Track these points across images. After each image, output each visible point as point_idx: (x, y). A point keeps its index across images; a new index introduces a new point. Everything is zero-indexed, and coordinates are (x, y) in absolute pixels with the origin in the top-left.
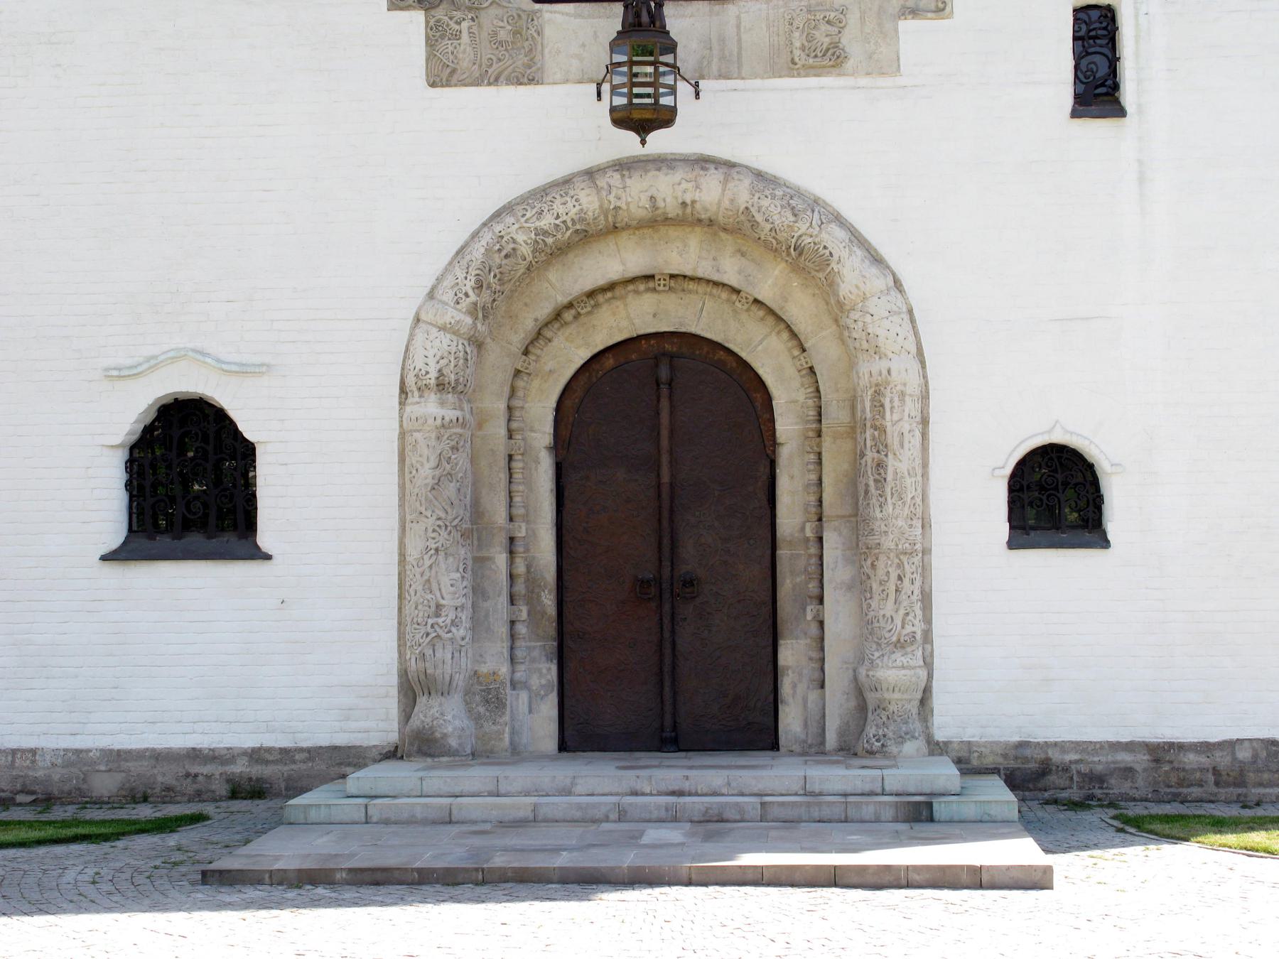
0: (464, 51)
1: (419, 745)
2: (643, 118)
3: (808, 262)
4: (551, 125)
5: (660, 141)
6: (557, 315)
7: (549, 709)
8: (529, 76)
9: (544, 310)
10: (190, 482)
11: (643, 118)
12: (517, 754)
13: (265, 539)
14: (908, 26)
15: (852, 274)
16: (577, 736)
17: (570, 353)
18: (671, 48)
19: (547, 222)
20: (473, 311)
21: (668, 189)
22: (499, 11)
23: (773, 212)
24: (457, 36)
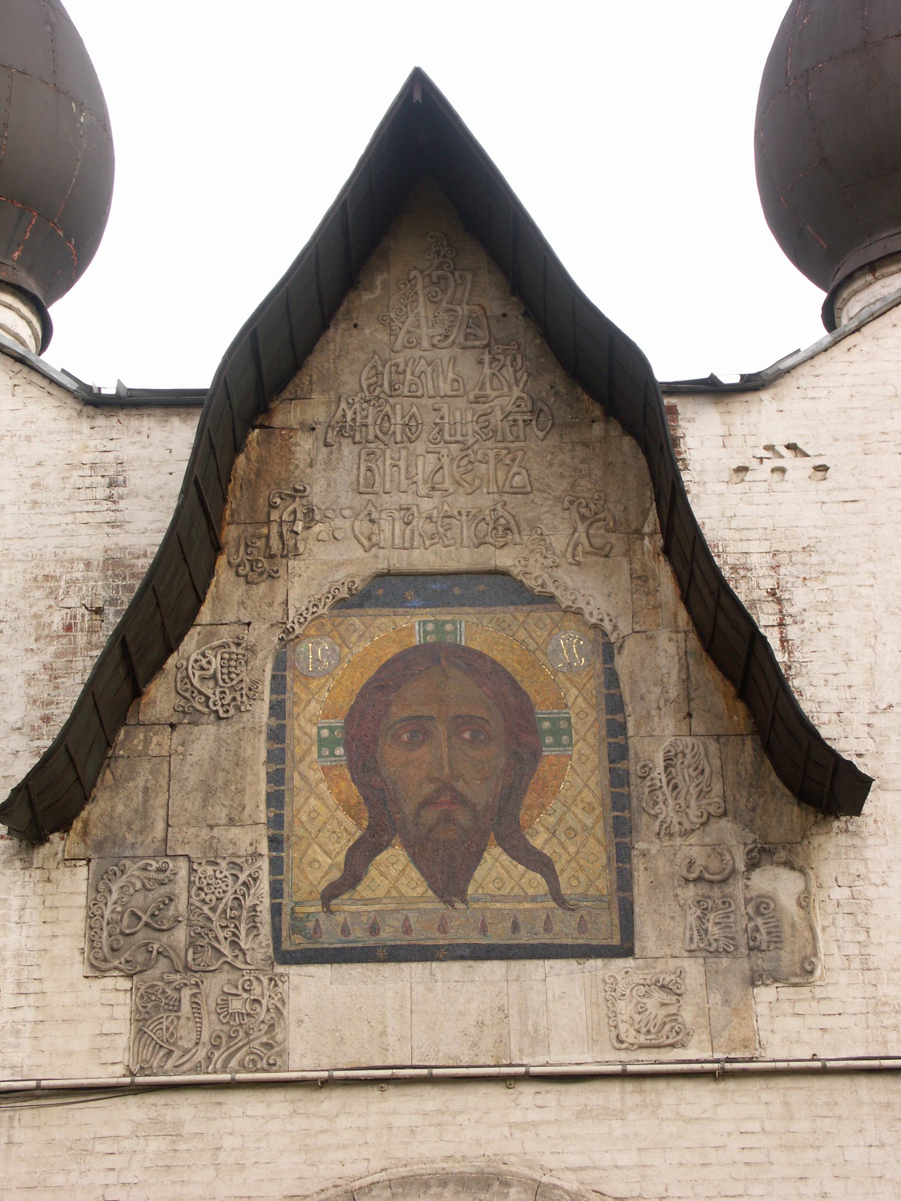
14: (765, 994)
22: (234, 976)
24: (176, 1007)
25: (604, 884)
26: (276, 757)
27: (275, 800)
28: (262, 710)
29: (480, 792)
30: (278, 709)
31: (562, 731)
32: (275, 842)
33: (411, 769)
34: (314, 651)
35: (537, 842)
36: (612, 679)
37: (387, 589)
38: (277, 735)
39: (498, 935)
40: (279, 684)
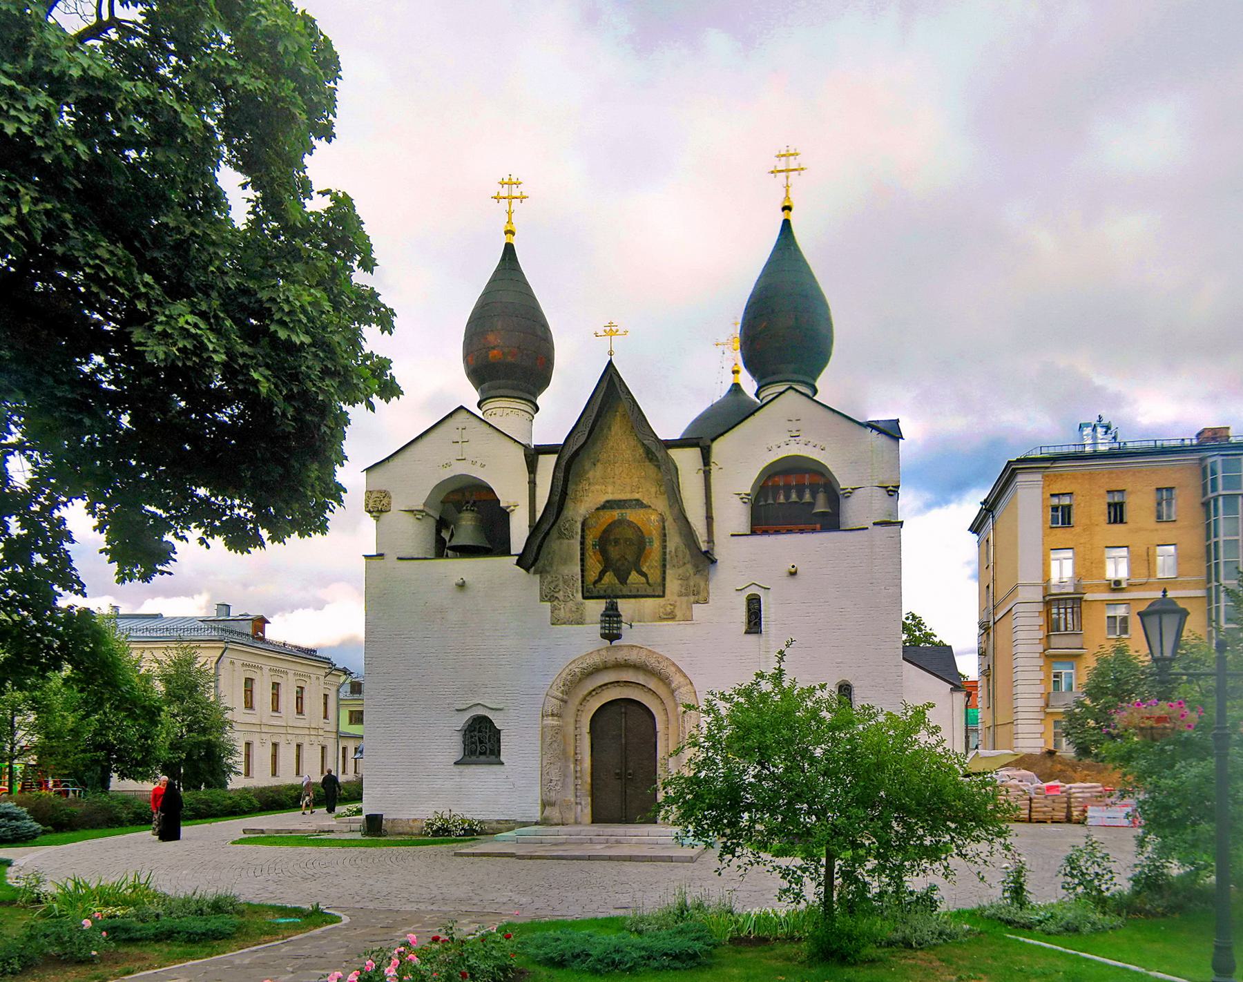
0: (562, 614)
1: (545, 822)
2: (611, 635)
3: (664, 680)
4: (582, 641)
5: (615, 643)
6: (590, 693)
7: (588, 810)
8: (580, 622)
9: (586, 692)
10: (481, 741)
11: (611, 635)
12: (577, 823)
13: (502, 759)
15: (677, 680)
16: (595, 820)
17: (595, 704)
18: (620, 616)
19: (585, 665)
20: (562, 692)
21: (621, 656)
23: (652, 662)
25: (659, 580)
26: (582, 549)
27: (582, 560)
28: (579, 537)
29: (630, 557)
30: (583, 537)
31: (651, 541)
32: (582, 571)
33: (614, 552)
34: (591, 522)
35: (644, 569)
36: (664, 528)
37: (609, 505)
38: (582, 543)
39: (634, 593)
40: (583, 530)
